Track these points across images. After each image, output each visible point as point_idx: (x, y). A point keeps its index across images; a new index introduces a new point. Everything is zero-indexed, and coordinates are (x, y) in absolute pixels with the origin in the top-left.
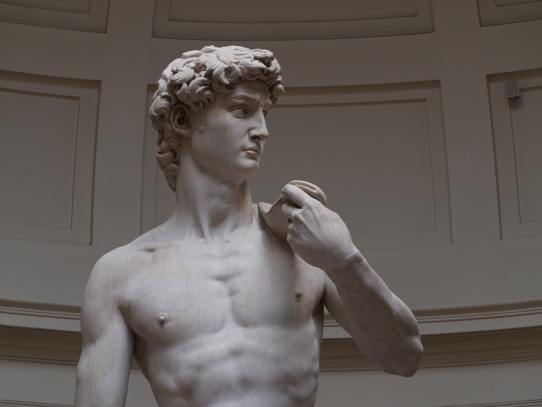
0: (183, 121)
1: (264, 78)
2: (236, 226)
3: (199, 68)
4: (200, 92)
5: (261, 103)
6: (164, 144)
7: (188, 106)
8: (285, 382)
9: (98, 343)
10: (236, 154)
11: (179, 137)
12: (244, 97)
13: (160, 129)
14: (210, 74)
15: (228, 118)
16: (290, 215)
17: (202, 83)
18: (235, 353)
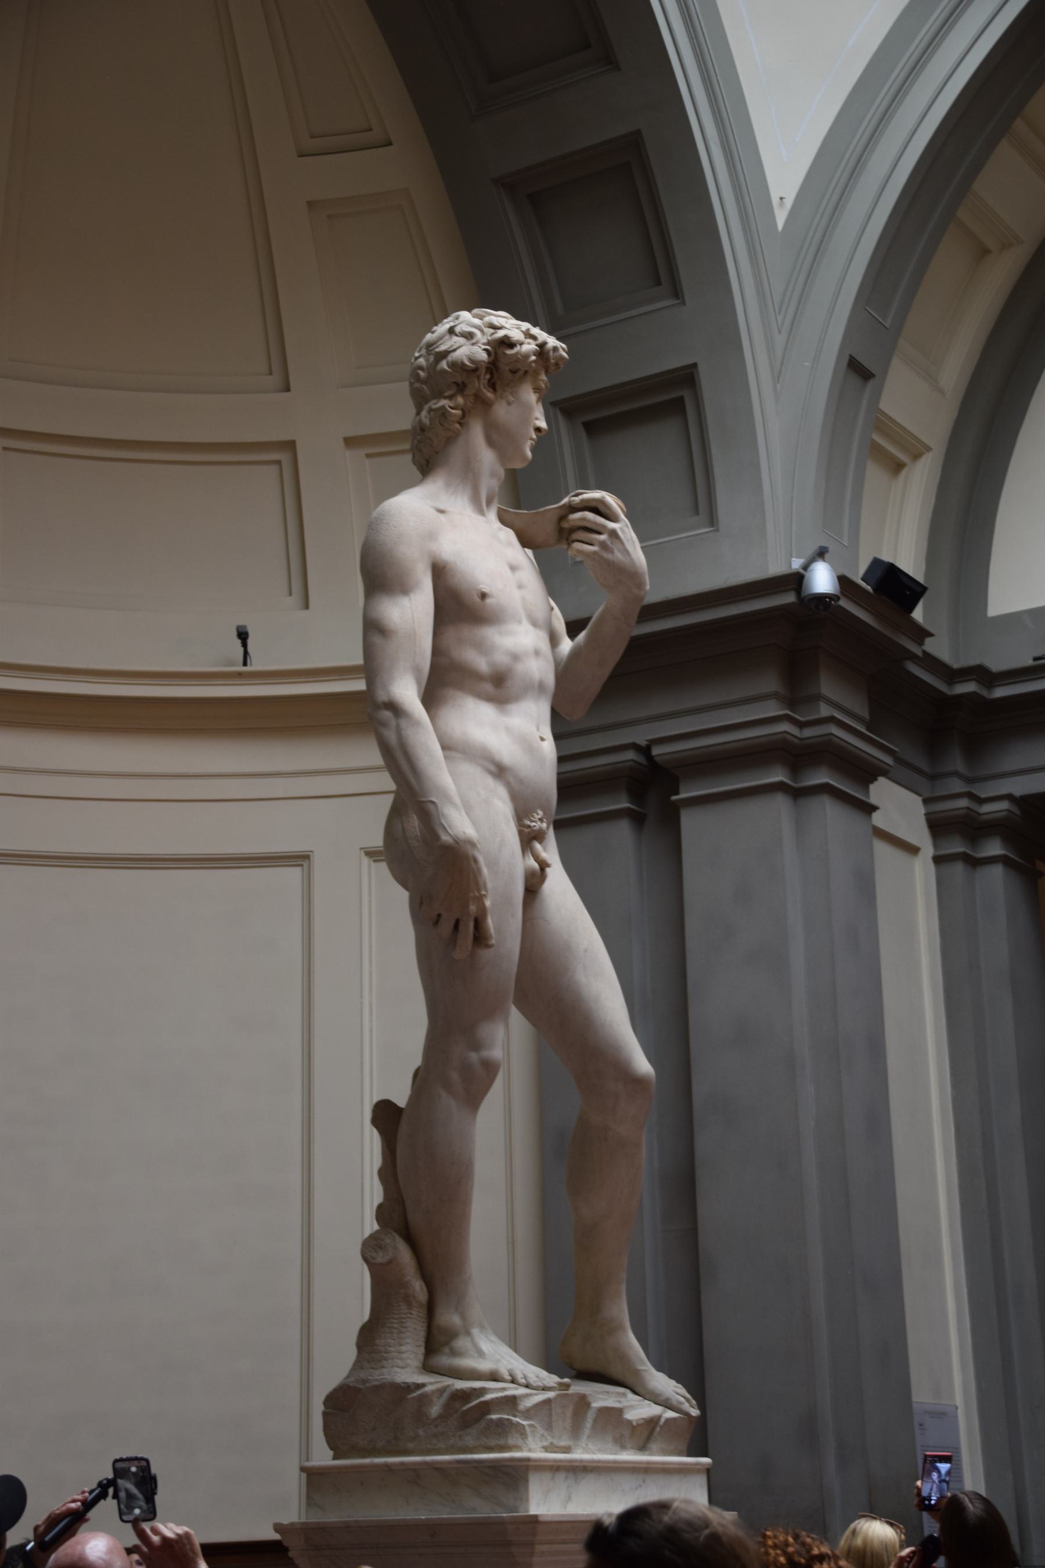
6: (460, 400)
9: (412, 595)
11: (478, 398)
13: (459, 380)
14: (542, 346)
16: (604, 527)
18: (537, 653)
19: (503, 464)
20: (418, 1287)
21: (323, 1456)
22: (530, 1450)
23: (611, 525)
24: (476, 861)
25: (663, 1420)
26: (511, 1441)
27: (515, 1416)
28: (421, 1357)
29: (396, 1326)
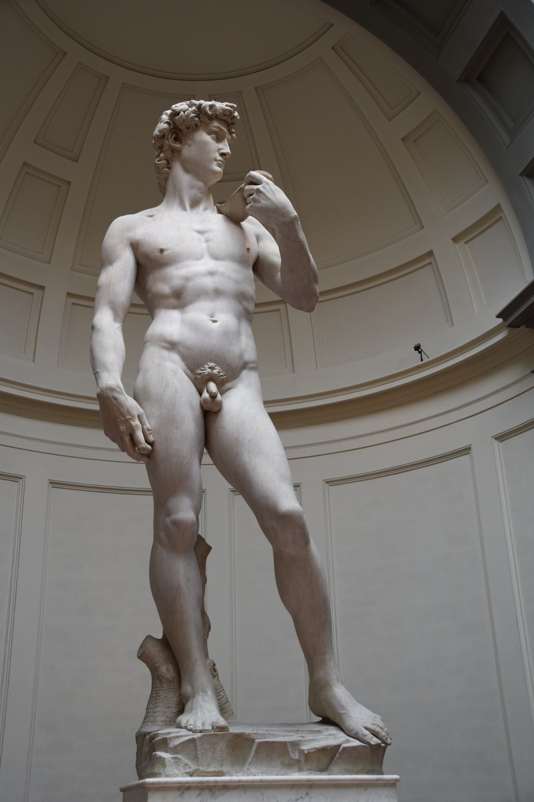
0: (176, 139)
1: (229, 121)
2: (205, 209)
3: (190, 106)
4: (192, 117)
5: (227, 135)
6: (162, 155)
7: (180, 130)
8: (241, 297)
9: (114, 264)
10: (211, 162)
12: (218, 127)
13: (161, 146)
14: (199, 107)
15: (208, 138)
16: (253, 189)
17: (194, 112)
18: (212, 273)
19: (202, 181)
20: (166, 670)
21: (136, 781)
22: (167, 776)
23: (256, 187)
24: (115, 399)
25: (341, 748)
26: (156, 770)
27: (167, 752)
28: (173, 715)
29: (155, 695)
